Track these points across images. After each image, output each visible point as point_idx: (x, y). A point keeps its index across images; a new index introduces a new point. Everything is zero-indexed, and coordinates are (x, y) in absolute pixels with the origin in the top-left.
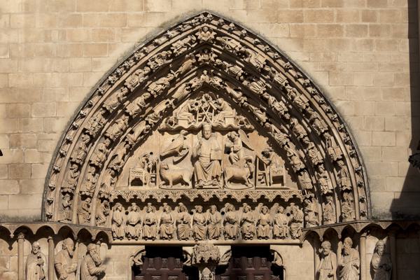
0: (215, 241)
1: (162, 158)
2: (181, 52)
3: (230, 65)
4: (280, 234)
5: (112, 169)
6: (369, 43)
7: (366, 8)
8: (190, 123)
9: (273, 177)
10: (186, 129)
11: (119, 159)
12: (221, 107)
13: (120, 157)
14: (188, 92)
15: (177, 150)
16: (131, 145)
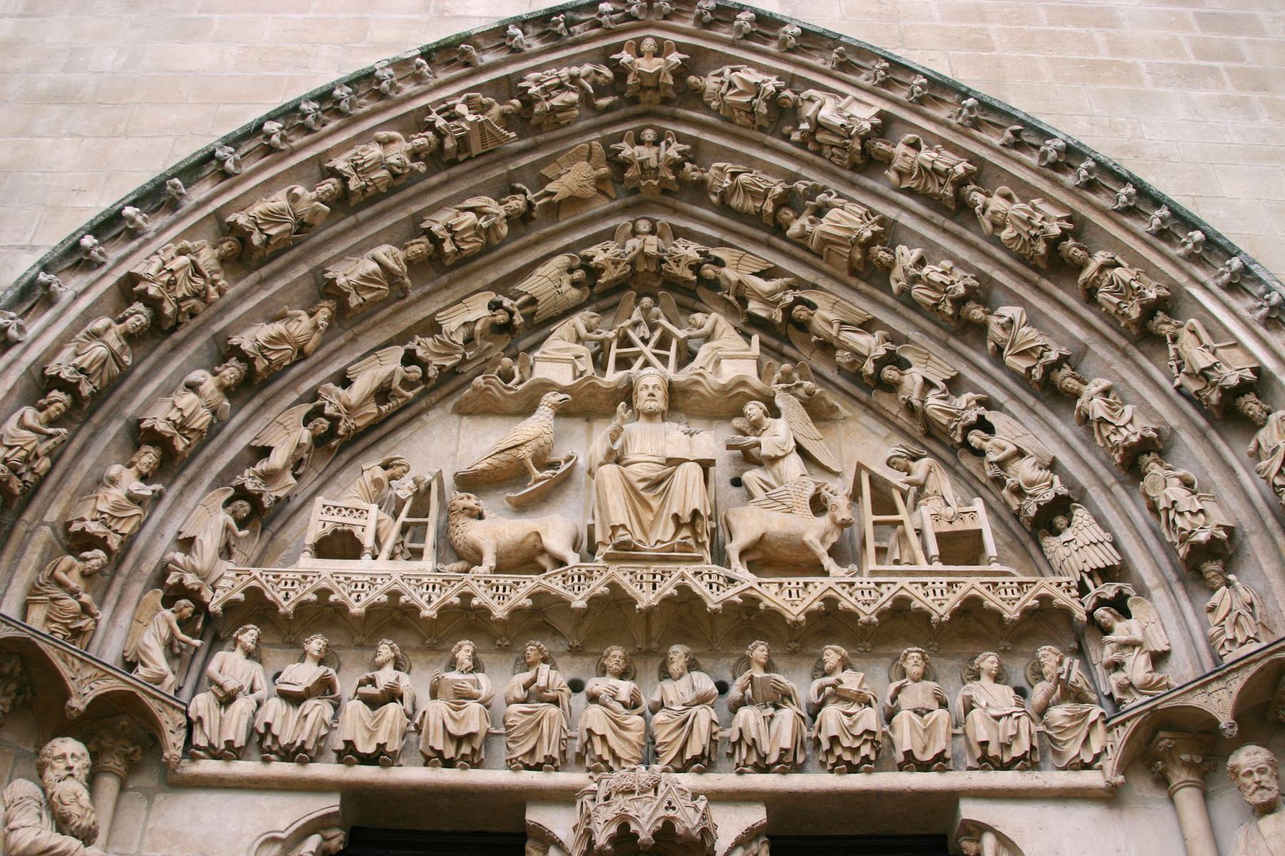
0: (688, 780)
1: (470, 482)
2: (556, 102)
3: (740, 168)
4: (1006, 747)
5: (241, 493)
6: (1240, 104)
7: (1199, 33)
8: (578, 374)
9: (940, 537)
10: (563, 390)
11: (278, 459)
12: (707, 328)
13: (278, 459)
14: (575, 292)
15: (525, 453)
16: (334, 420)
